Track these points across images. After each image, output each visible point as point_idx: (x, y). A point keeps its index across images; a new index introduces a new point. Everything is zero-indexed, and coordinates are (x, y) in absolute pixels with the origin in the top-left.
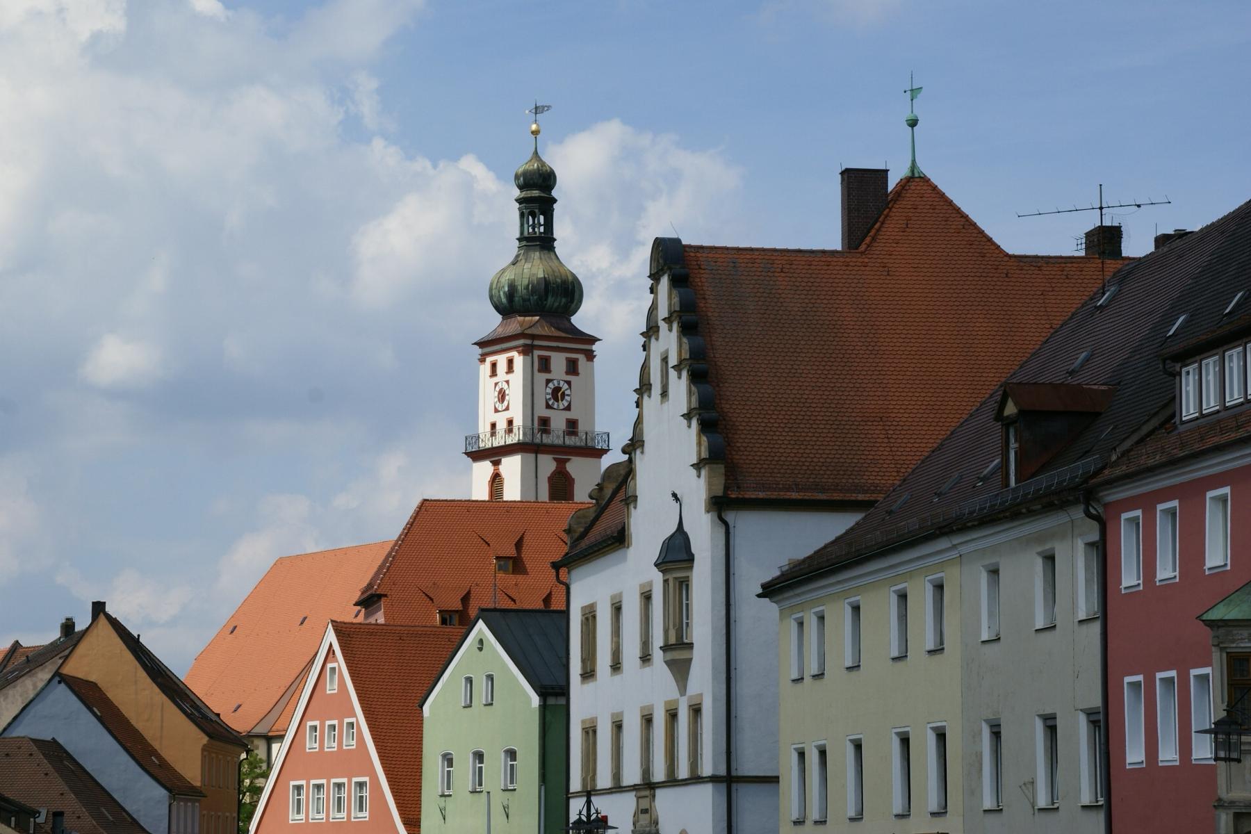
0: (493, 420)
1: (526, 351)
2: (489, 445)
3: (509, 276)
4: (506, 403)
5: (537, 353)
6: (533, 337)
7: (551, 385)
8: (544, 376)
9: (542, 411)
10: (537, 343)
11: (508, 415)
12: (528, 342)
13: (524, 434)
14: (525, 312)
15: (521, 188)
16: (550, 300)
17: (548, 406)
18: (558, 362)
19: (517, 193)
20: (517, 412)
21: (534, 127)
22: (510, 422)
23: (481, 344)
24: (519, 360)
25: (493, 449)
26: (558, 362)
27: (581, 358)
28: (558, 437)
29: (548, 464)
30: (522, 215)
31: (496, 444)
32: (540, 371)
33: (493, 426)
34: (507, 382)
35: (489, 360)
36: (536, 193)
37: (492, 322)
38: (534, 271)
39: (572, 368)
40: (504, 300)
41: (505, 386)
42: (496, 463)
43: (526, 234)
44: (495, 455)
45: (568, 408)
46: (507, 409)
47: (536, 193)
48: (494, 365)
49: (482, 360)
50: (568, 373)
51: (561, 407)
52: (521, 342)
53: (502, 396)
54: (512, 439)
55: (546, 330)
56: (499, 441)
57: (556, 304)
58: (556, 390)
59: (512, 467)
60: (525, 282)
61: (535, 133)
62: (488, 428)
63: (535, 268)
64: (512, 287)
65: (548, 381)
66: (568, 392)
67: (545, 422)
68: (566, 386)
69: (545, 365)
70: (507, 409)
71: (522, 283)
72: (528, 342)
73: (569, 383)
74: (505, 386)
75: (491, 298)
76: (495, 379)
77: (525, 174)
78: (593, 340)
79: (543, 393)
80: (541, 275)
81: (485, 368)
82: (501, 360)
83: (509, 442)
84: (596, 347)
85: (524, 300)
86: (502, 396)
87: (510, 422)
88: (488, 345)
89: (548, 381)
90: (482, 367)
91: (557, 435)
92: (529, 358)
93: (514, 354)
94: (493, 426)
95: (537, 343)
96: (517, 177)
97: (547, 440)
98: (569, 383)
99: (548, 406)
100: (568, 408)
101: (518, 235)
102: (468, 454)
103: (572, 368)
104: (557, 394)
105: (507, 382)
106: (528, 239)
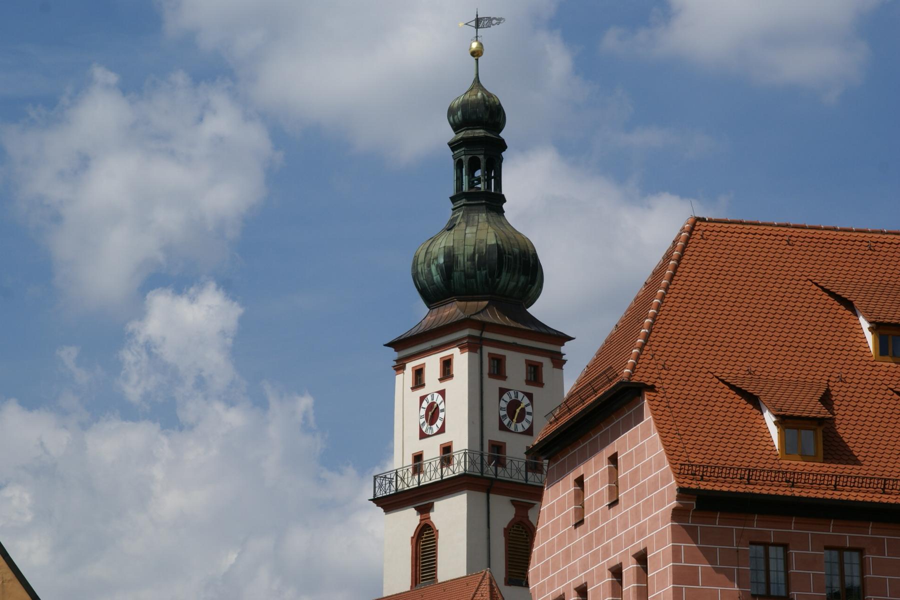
0: (416, 450)
1: (472, 345)
2: (414, 484)
3: (446, 241)
4: (439, 423)
5: (487, 350)
6: (483, 326)
7: (506, 397)
8: (492, 385)
9: (494, 434)
10: (487, 335)
11: (443, 439)
12: (476, 333)
13: (472, 462)
14: (466, 293)
15: (456, 127)
16: (505, 277)
17: (502, 427)
18: (516, 365)
19: (450, 135)
20: (459, 434)
21: (474, 45)
22: (447, 449)
23: (397, 344)
24: (461, 360)
25: (420, 488)
26: (516, 365)
27: (546, 362)
28: (518, 470)
29: (504, 511)
30: (459, 165)
31: (425, 480)
32: (491, 375)
33: (418, 458)
34: (442, 393)
35: (410, 366)
36: (480, 132)
37: (418, 314)
38: (482, 235)
39: (535, 376)
40: (437, 277)
41: (438, 399)
42: (425, 510)
43: (465, 188)
44: (421, 498)
46: (442, 430)
47: (480, 132)
48: (419, 373)
49: (400, 367)
50: (528, 382)
51: (520, 429)
52: (466, 332)
53: (433, 413)
54: (458, 468)
55: (498, 319)
56: (432, 474)
57: (512, 284)
58: (514, 405)
59: (452, 515)
60: (470, 250)
61: (476, 54)
62: (409, 461)
63: (479, 234)
64: (450, 256)
65: (502, 391)
67: (498, 448)
68: (526, 401)
69: (498, 369)
70: (442, 430)
71: (464, 252)
72: (476, 333)
74: (438, 399)
75: (415, 276)
76: (421, 392)
77: (465, 106)
78: (562, 338)
79: (495, 408)
80: (492, 241)
81: (406, 378)
82: (432, 364)
83: (448, 473)
84: (566, 349)
85: (467, 276)
86: (433, 413)
87: (447, 449)
88: (408, 345)
89: (502, 391)
90: (399, 378)
92: (476, 356)
93: (455, 351)
94: (418, 458)
95: (487, 335)
96: (451, 112)
97: (503, 474)
98: (530, 396)
99: (502, 427)
101: (452, 192)
102: (377, 501)
103: (535, 376)
105: (442, 393)
106: (467, 196)
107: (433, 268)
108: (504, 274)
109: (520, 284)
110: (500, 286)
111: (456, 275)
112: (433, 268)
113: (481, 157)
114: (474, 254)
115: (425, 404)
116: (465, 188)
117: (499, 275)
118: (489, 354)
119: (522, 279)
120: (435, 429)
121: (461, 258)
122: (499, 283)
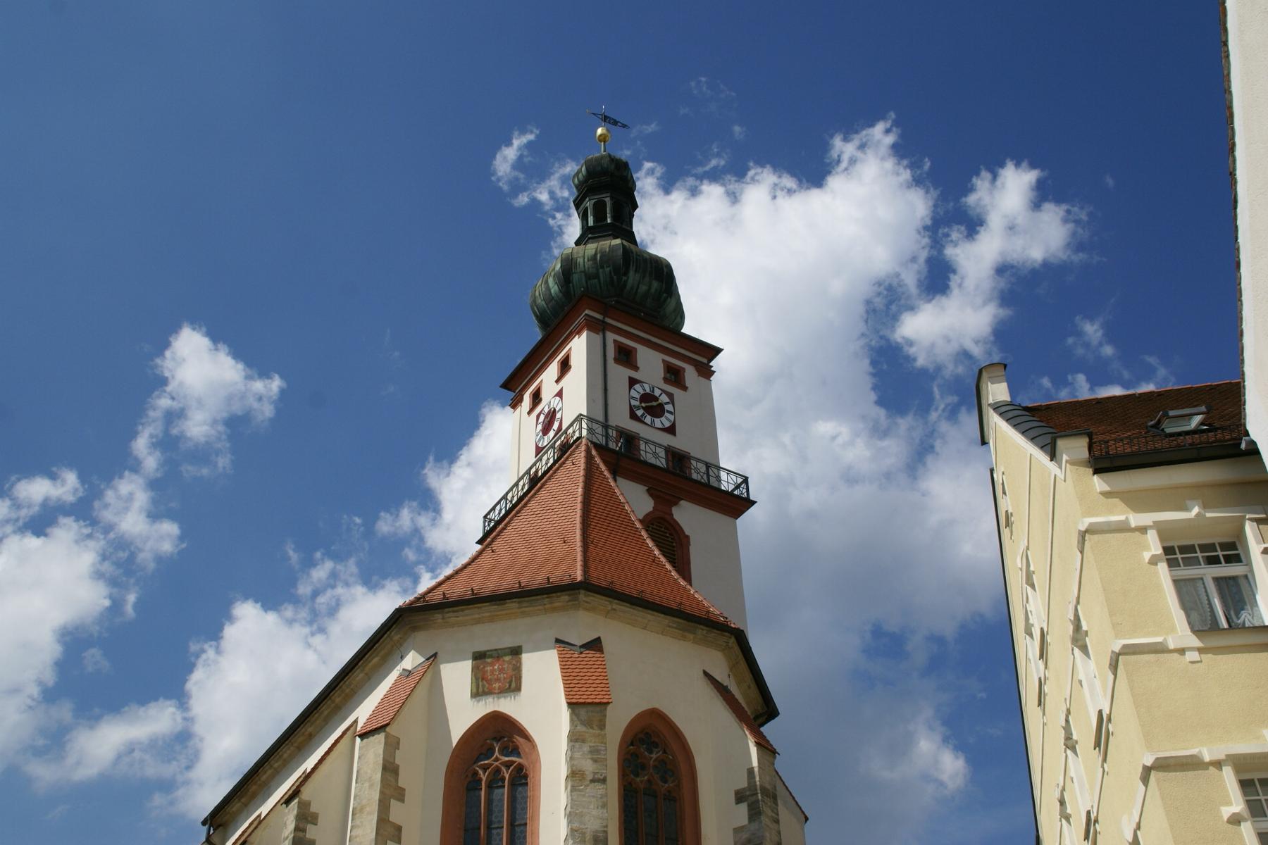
5: (611, 337)
7: (637, 387)
8: (619, 374)
9: (621, 419)
27: (690, 373)
28: (656, 455)
39: (674, 376)
40: (554, 289)
45: (671, 430)
51: (658, 425)
57: (643, 288)
65: (633, 382)
66: (669, 407)
68: (664, 399)
69: (626, 357)
73: (671, 396)
85: (588, 276)
89: (633, 382)
98: (671, 396)
99: (633, 416)
100: (671, 430)
105: (560, 394)
107: (551, 281)
108: (631, 273)
109: (653, 290)
110: (628, 287)
111: (575, 277)
112: (551, 281)
113: (607, 200)
114: (596, 254)
115: (542, 417)
116: (591, 223)
117: (626, 273)
118: (615, 341)
119: (655, 284)
121: (580, 260)
122: (626, 282)
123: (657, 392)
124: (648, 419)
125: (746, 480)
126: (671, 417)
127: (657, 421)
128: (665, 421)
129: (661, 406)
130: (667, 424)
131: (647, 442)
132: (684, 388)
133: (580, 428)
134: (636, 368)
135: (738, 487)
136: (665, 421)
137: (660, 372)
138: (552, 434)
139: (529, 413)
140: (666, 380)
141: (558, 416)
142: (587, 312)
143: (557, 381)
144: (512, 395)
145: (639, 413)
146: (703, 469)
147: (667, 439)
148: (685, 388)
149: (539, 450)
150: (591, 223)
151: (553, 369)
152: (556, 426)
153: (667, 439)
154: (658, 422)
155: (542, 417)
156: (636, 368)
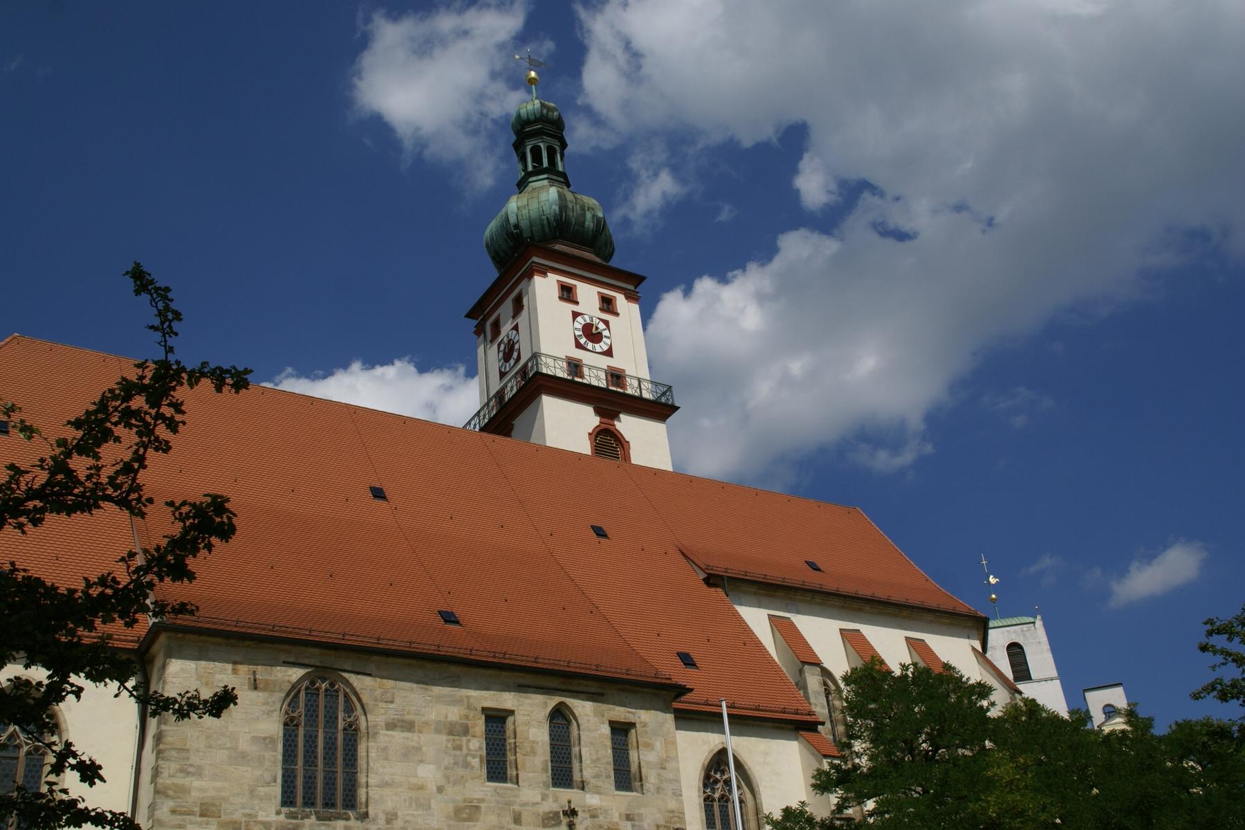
7: (579, 319)
27: (620, 300)
35: (489, 323)
46: (519, 358)
51: (598, 350)
65: (575, 315)
66: (606, 333)
68: (602, 326)
73: (606, 323)
89: (575, 315)
91: (595, 377)
98: (606, 323)
99: (579, 346)
100: (609, 353)
104: (590, 333)
105: (516, 328)
113: (542, 145)
115: (502, 347)
120: (512, 362)
123: (596, 321)
124: (590, 346)
125: (670, 388)
126: (608, 341)
127: (597, 346)
128: (603, 346)
129: (600, 334)
130: (606, 348)
131: (590, 367)
132: (617, 314)
133: (537, 364)
134: (577, 303)
135: (664, 394)
136: (603, 346)
137: (596, 303)
138: (512, 362)
139: (492, 341)
140: (601, 309)
141: (516, 347)
142: (535, 259)
143: (514, 317)
144: (475, 322)
145: (583, 341)
146: (635, 383)
147: (605, 362)
148: (617, 314)
149: (502, 375)
150: (530, 168)
151: (508, 306)
152: (515, 355)
153: (605, 362)
154: (598, 347)
155: (502, 347)
156: (577, 303)
